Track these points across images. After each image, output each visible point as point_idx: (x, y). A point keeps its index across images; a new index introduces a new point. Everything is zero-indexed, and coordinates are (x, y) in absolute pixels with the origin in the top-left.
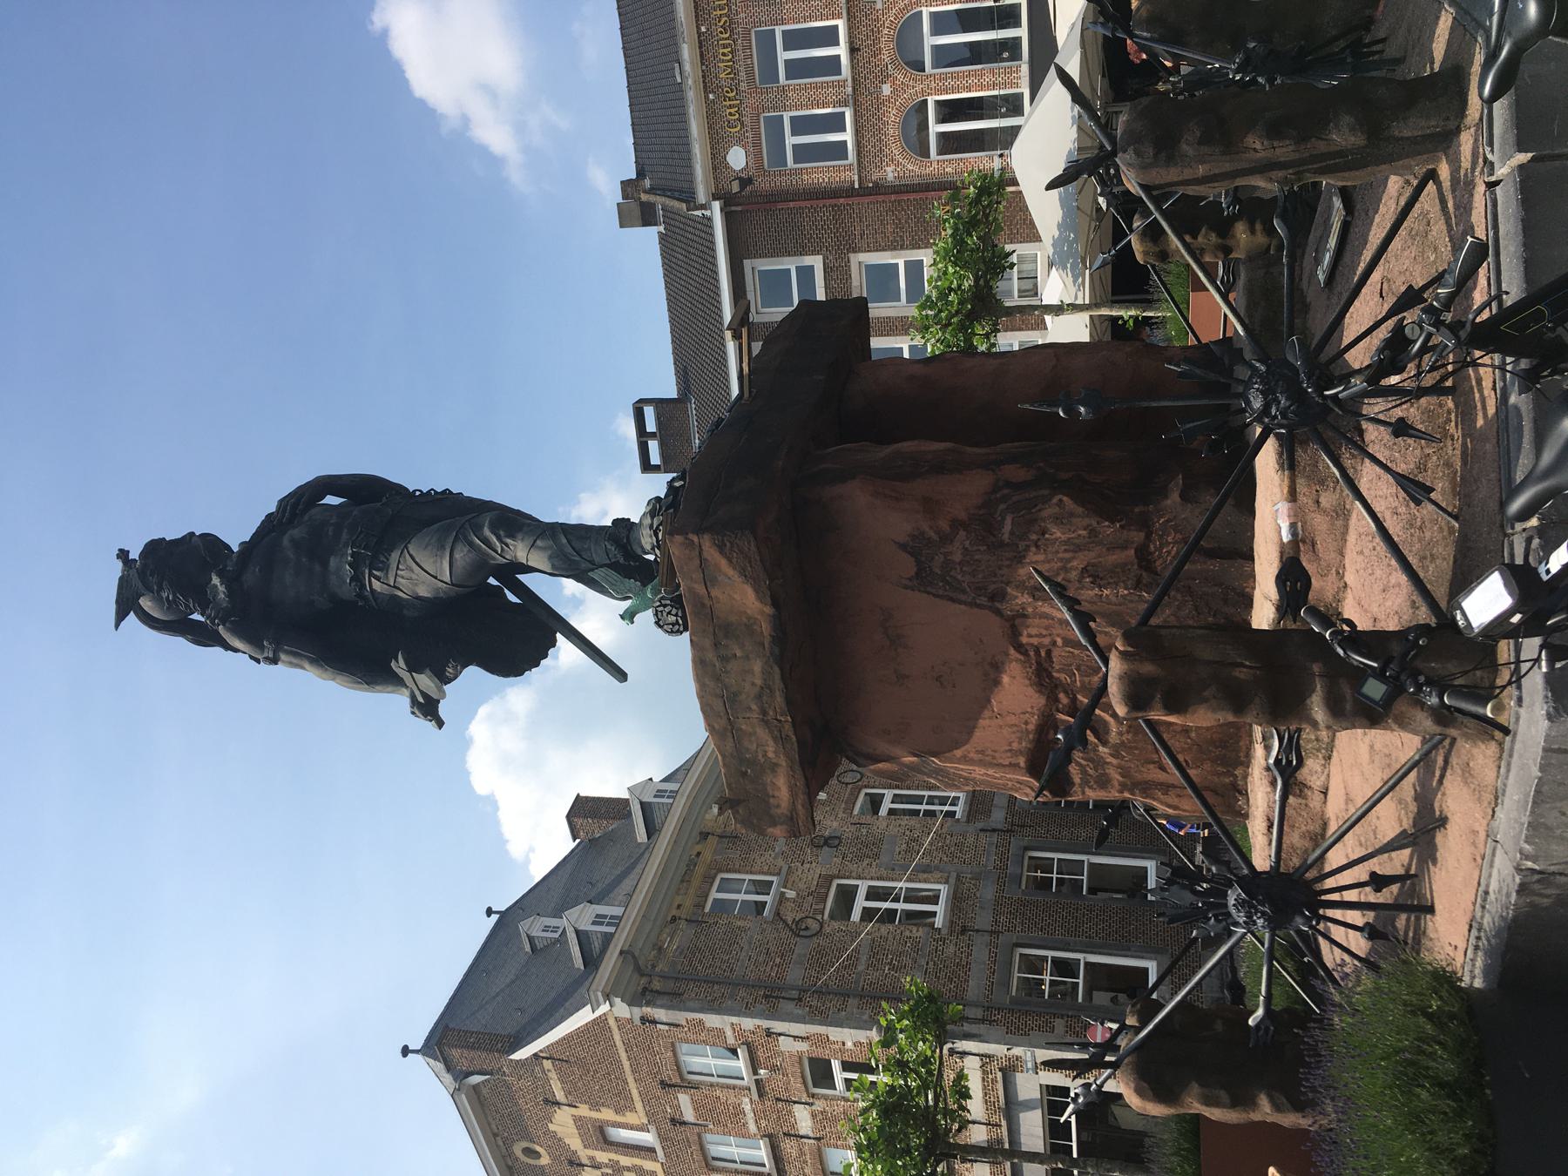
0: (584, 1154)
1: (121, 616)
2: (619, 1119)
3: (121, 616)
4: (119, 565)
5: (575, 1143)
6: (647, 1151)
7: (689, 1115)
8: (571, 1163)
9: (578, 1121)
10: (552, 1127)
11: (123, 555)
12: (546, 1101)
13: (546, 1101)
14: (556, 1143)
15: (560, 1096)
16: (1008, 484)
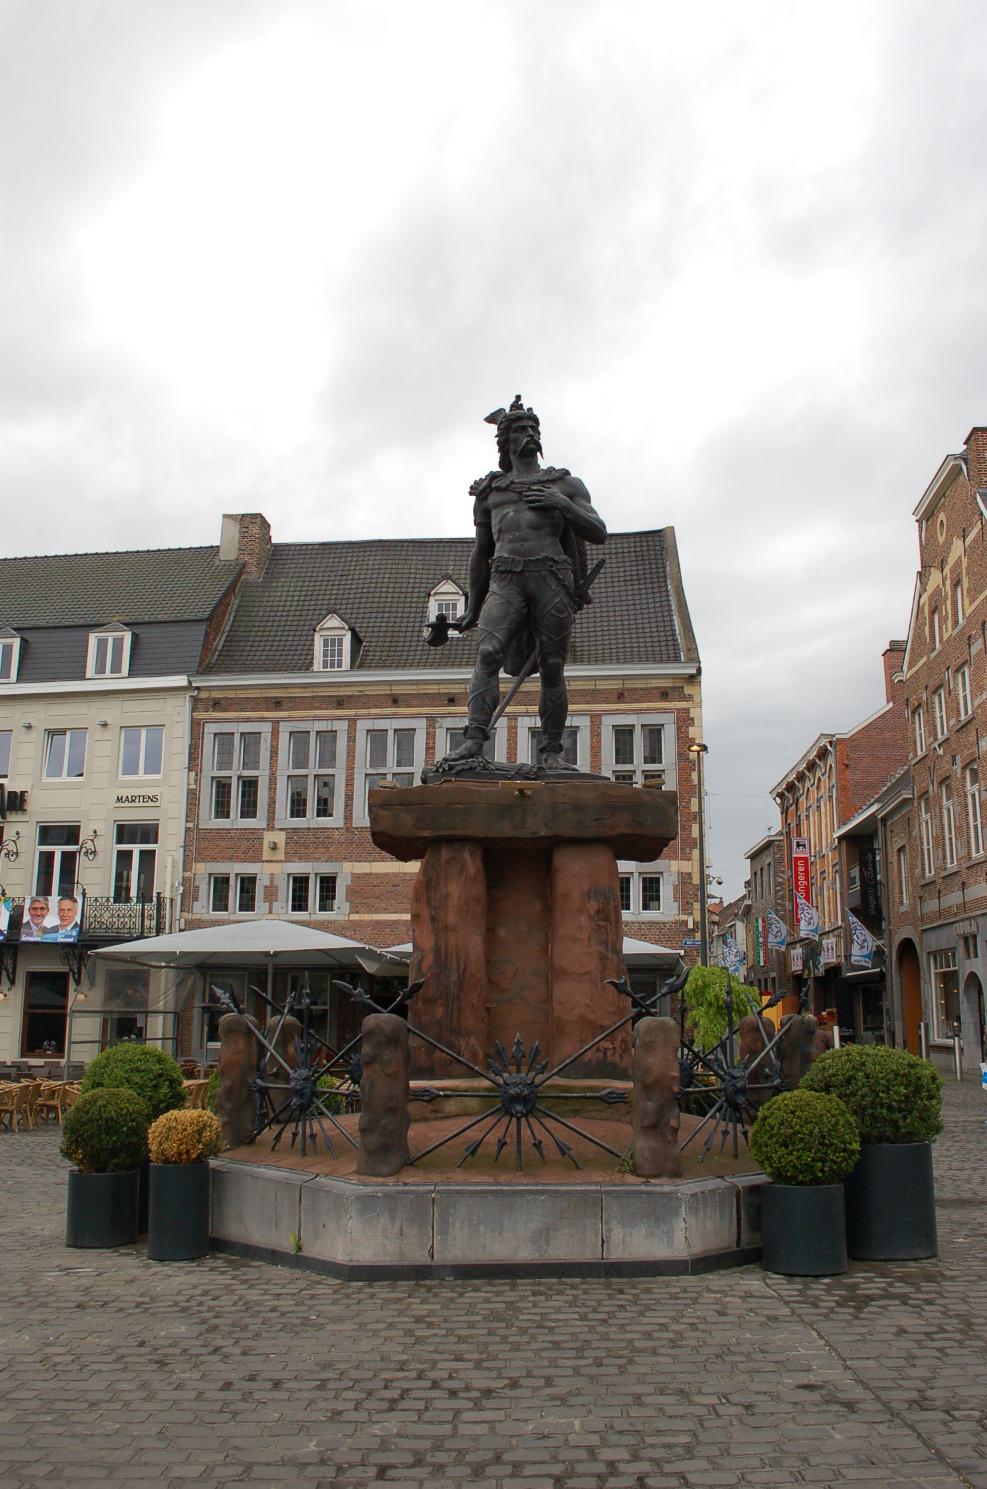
0: (947, 570)
1: (490, 419)
2: (965, 593)
3: (490, 419)
4: (514, 399)
5: (951, 561)
6: (956, 623)
7: (974, 650)
8: (942, 561)
9: (958, 562)
10: (954, 538)
11: (518, 398)
12: (964, 531)
13: (964, 531)
14: (949, 543)
15: (968, 540)
16: (423, 957)
